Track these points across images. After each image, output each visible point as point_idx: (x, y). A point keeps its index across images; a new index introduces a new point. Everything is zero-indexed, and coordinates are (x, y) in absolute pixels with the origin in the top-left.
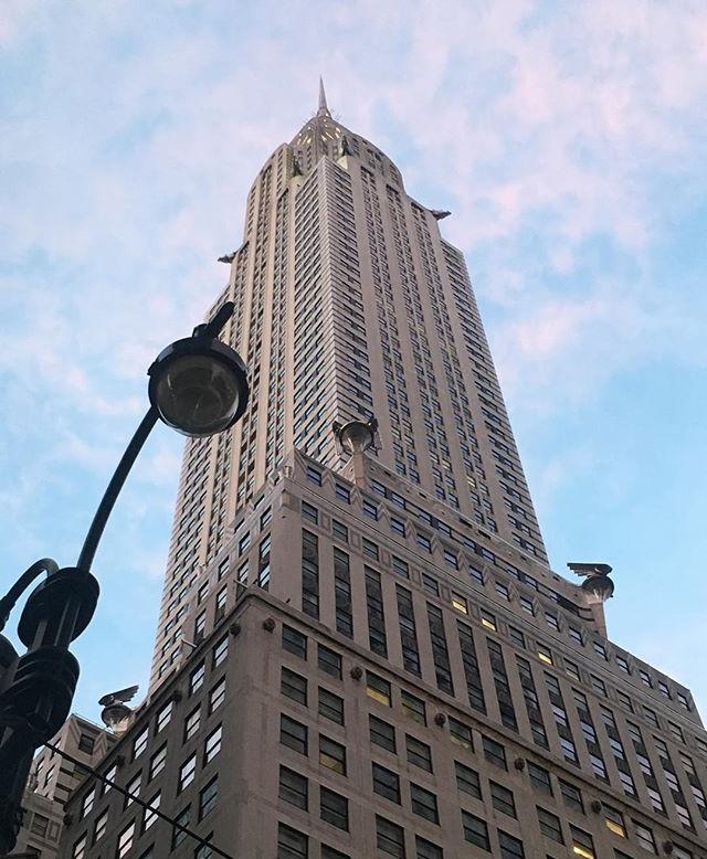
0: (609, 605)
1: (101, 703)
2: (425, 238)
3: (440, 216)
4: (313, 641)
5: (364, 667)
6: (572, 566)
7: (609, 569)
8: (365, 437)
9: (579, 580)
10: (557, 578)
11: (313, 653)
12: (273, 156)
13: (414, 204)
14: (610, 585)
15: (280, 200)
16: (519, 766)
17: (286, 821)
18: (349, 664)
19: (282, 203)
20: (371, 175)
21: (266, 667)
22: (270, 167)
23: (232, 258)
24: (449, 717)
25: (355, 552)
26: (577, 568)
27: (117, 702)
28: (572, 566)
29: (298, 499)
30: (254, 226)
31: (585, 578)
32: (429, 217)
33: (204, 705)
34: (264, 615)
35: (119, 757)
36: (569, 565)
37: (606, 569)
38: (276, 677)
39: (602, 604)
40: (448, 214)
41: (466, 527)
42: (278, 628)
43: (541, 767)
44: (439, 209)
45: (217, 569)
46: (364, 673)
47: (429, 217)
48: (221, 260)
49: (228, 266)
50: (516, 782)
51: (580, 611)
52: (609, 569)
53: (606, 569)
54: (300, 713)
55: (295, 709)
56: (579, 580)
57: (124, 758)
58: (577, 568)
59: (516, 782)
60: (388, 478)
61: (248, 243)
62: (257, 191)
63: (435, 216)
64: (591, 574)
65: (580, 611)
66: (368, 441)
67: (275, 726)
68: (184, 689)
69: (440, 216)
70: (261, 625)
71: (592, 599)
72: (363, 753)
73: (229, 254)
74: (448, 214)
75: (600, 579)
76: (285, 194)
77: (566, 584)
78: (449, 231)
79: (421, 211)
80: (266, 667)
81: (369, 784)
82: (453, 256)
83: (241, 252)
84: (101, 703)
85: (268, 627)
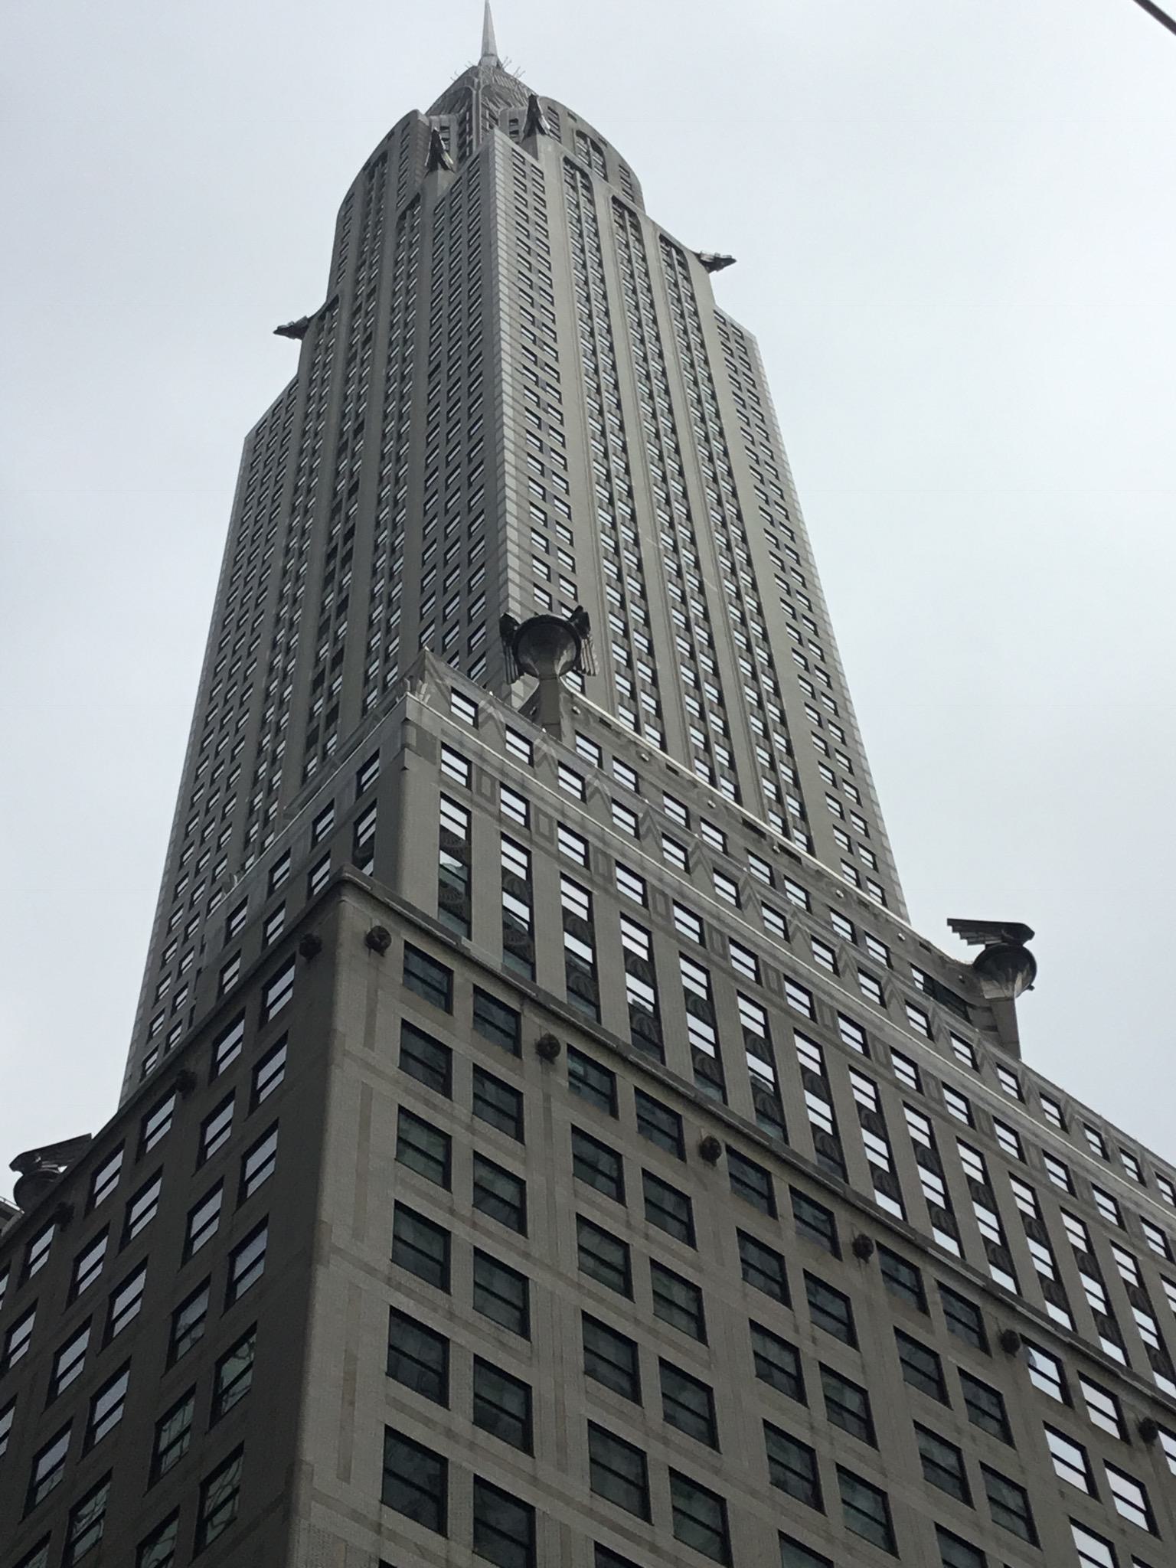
0: (1024, 1003)
1: (14, 1166)
2: (689, 309)
3: (717, 263)
4: (463, 979)
5: (565, 1038)
6: (960, 926)
8: (564, 647)
9: (966, 953)
10: (926, 946)
11: (464, 1004)
12: (391, 135)
13: (665, 240)
14: (1027, 965)
15: (403, 217)
16: (862, 1249)
17: (408, 1307)
18: (534, 1027)
20: (584, 175)
21: (371, 1014)
23: (307, 327)
24: (729, 1149)
25: (542, 848)
26: (965, 928)
27: (46, 1166)
28: (957, 925)
29: (435, 738)
31: (980, 948)
33: (244, 1094)
34: (377, 920)
35: (62, 1205)
36: (952, 922)
37: (1022, 932)
38: (391, 1039)
39: (1012, 999)
40: (729, 261)
41: (755, 835)
42: (396, 949)
43: (899, 1256)
44: (710, 249)
45: (265, 876)
46: (564, 1049)
47: (694, 266)
48: (281, 331)
49: (298, 342)
50: (857, 1280)
51: (969, 1010)
53: (1022, 932)
54: (435, 1107)
55: (427, 1102)
56: (966, 953)
57: (72, 1208)
58: (965, 928)
59: (857, 1280)
60: (605, 731)
62: (358, 204)
63: (704, 263)
65: (969, 1010)
66: (566, 657)
67: (386, 1130)
68: (198, 1066)
69: (717, 263)
70: (362, 937)
71: (990, 991)
72: (556, 1193)
73: (296, 318)
74: (729, 261)
75: (1007, 950)
76: (412, 206)
77: (943, 960)
78: (724, 292)
79: (679, 252)
80: (371, 1014)
81: (570, 1258)
82: (739, 345)
84: (14, 1166)
85: (376, 942)
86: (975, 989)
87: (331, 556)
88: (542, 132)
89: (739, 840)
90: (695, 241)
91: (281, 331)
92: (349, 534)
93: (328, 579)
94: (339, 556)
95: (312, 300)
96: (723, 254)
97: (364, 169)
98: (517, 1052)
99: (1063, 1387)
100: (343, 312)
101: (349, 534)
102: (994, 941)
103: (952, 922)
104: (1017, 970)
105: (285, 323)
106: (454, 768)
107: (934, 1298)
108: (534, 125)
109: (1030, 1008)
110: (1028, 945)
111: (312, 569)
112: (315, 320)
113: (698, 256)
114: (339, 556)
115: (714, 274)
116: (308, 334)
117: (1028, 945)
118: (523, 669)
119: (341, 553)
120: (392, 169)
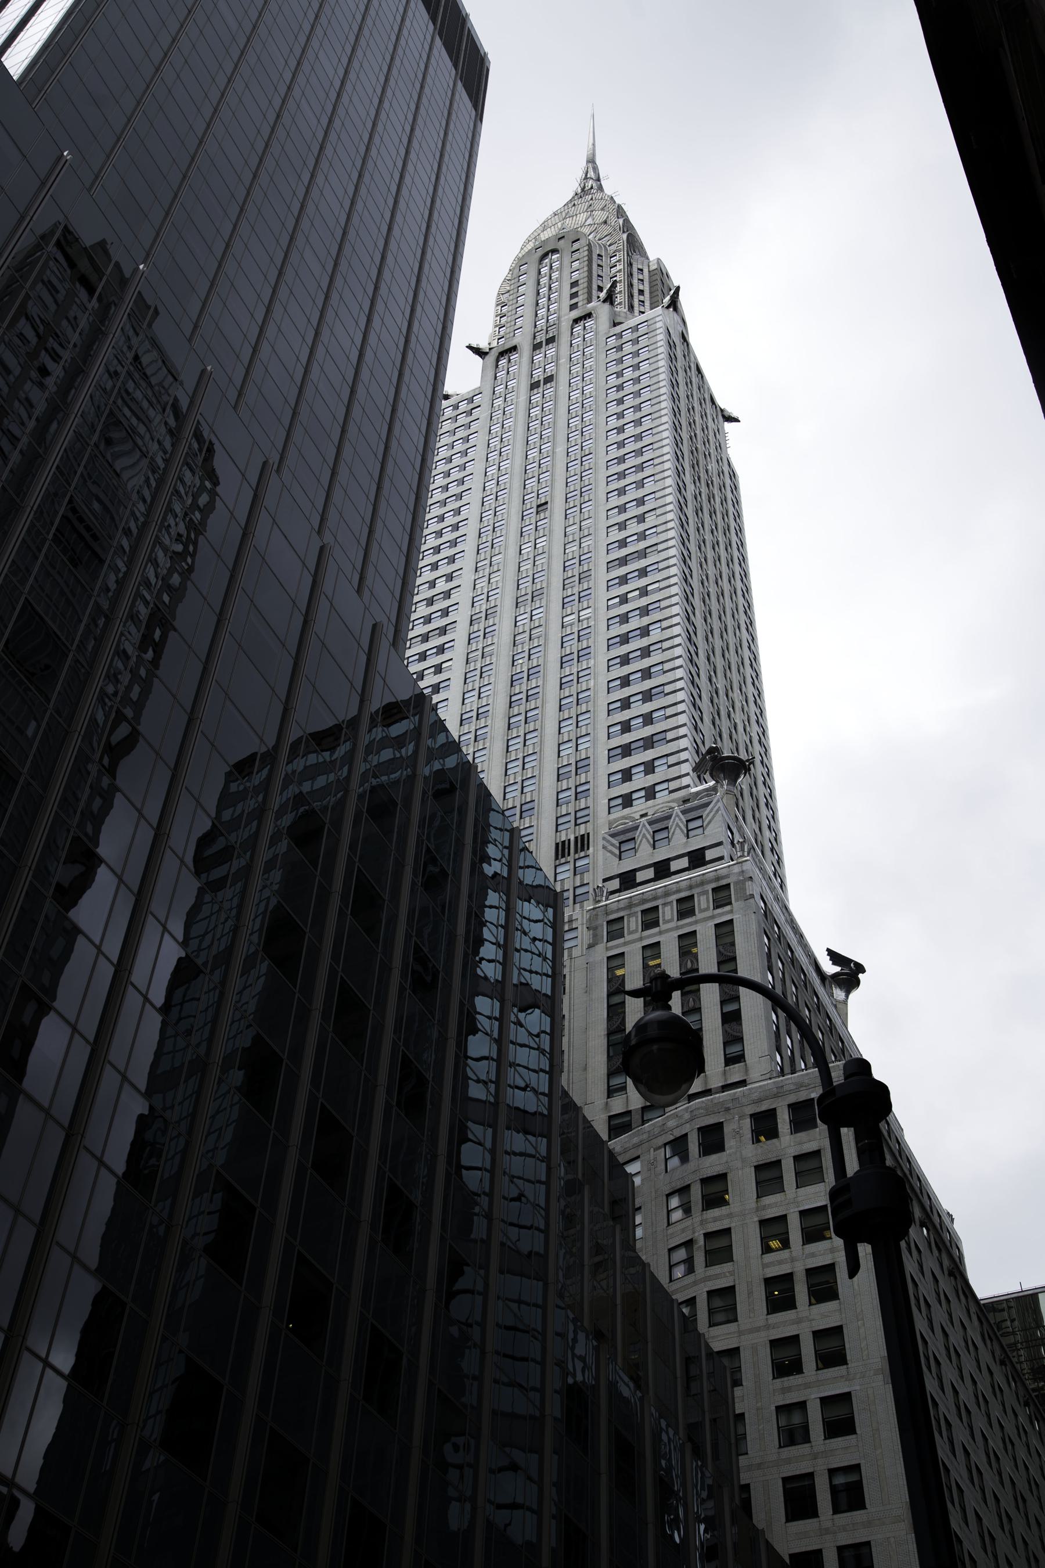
6: (831, 953)
7: (863, 971)
9: (830, 968)
14: (857, 983)
15: (576, 321)
28: (831, 953)
31: (838, 969)
36: (828, 950)
37: (860, 968)
40: (736, 420)
44: (732, 410)
48: (470, 347)
52: (863, 971)
56: (830, 968)
58: (835, 957)
74: (736, 420)
75: (850, 974)
91: (470, 347)
103: (828, 950)
110: (860, 976)
113: (722, 411)
117: (860, 976)
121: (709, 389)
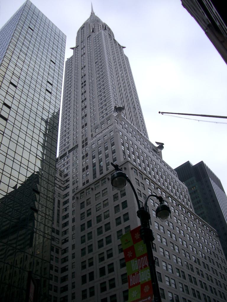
3: (124, 47)
7: (164, 144)
9: (157, 146)
10: (153, 145)
11: (138, 174)
13: (119, 45)
14: (163, 147)
15: (88, 37)
19: (88, 39)
22: (84, 27)
26: (157, 143)
30: (80, 41)
31: (158, 145)
32: (122, 48)
37: (163, 144)
40: (125, 47)
44: (124, 46)
47: (122, 48)
48: (71, 48)
49: (73, 50)
52: (164, 144)
56: (157, 146)
58: (157, 143)
61: (78, 46)
64: (160, 145)
69: (124, 47)
71: (159, 150)
74: (125, 47)
75: (161, 146)
76: (89, 36)
77: (155, 147)
82: (127, 58)
83: (76, 48)
85: (132, 169)
86: (157, 150)
87: (82, 84)
88: (106, 30)
89: (137, 134)
90: (122, 45)
91: (71, 48)
92: (85, 82)
93: (82, 87)
94: (84, 84)
95: (74, 45)
96: (125, 46)
97: (81, 28)
98: (143, 179)
99: (161, 192)
100: (80, 48)
101: (85, 82)
102: (160, 145)
104: (162, 148)
105: (71, 47)
106: (121, 134)
107: (138, 174)
108: (105, 29)
109: (163, 152)
110: (163, 145)
111: (80, 86)
112: (75, 48)
113: (122, 46)
114: (84, 84)
115: (124, 49)
116: (75, 49)
117: (163, 145)
118: (116, 111)
119: (84, 84)
120: (85, 29)
121: (118, 43)
